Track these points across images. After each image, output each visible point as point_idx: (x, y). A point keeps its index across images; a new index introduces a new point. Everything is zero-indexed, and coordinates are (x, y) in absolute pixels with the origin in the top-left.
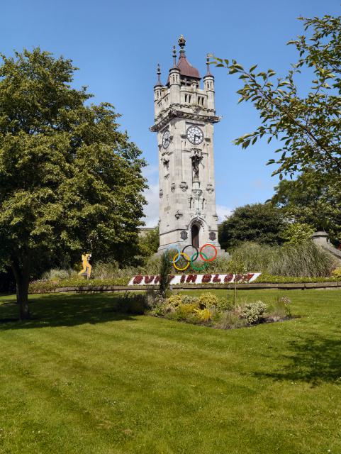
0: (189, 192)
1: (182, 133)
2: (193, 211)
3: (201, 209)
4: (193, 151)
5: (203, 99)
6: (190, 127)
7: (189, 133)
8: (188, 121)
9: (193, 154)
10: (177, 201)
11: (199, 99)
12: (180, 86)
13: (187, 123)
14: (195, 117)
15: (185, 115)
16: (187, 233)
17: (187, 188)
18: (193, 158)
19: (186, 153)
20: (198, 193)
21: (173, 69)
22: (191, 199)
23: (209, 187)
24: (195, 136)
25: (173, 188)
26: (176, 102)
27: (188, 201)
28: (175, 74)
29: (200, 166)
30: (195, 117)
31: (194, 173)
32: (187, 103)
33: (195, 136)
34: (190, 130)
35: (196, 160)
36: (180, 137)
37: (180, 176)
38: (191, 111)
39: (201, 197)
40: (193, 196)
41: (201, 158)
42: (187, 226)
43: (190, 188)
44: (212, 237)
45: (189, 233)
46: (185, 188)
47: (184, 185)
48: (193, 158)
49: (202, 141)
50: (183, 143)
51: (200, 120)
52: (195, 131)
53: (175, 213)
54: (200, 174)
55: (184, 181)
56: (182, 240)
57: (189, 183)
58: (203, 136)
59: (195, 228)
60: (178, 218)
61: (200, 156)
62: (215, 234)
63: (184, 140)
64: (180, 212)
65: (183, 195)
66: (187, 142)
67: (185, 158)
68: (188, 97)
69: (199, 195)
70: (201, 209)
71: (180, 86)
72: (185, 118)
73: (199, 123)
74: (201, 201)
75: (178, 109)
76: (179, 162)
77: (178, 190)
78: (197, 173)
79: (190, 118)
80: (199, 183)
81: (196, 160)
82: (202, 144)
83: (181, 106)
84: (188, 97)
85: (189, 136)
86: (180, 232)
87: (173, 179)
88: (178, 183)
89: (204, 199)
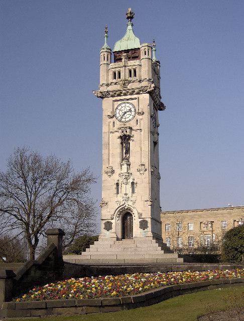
0: (116, 177)
3: (130, 194)
7: (118, 111)
9: (119, 134)
17: (113, 172)
18: (121, 137)
20: (124, 177)
32: (114, 81)
34: (120, 108)
35: (125, 139)
38: (118, 87)
41: (129, 137)
45: (116, 223)
50: (111, 124)
63: (112, 120)
69: (127, 179)
72: (113, 96)
79: (119, 95)
81: (125, 139)
89: (133, 183)
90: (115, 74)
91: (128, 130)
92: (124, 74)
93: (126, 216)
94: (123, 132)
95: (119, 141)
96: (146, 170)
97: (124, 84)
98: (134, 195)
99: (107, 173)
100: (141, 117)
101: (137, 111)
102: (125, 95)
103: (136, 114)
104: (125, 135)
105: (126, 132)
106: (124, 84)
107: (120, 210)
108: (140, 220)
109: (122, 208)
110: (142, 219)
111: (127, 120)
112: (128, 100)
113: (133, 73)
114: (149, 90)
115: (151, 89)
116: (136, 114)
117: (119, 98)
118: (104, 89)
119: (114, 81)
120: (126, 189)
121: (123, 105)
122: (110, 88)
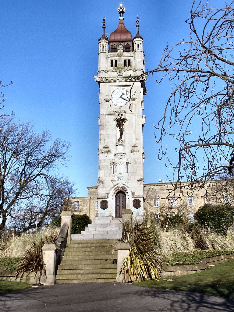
0: (111, 157)
4: (117, 114)
5: (129, 61)
17: (109, 152)
18: (117, 120)
19: (110, 116)
35: (120, 122)
38: (115, 74)
48: (117, 120)
57: (112, 147)
62: (139, 201)
65: (104, 160)
72: (109, 82)
79: (115, 81)
81: (120, 122)
90: (112, 61)
92: (121, 63)
93: (121, 193)
94: (119, 115)
95: (115, 123)
97: (120, 72)
99: (104, 153)
105: (122, 115)
108: (133, 199)
109: (118, 187)
110: (135, 198)
112: (123, 86)
113: (128, 63)
118: (103, 75)
119: (112, 68)
120: (121, 168)
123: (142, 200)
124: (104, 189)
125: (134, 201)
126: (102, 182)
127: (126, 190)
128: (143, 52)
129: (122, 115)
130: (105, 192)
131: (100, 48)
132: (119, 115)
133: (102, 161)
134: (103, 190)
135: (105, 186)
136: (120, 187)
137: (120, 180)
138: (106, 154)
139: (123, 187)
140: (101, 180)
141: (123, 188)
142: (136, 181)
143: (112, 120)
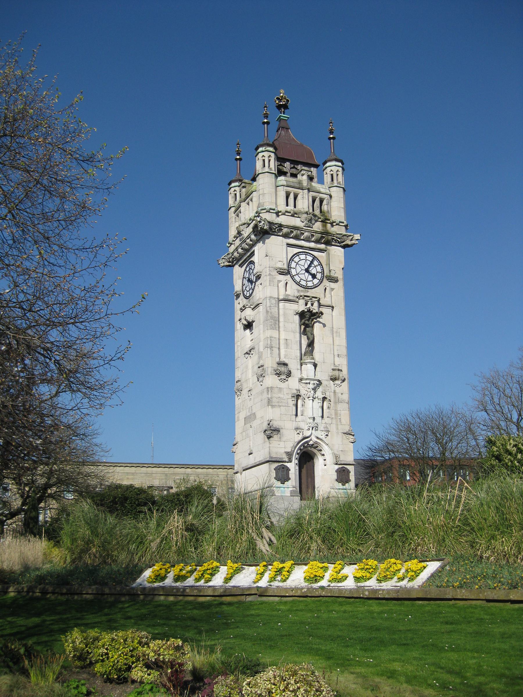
0: (293, 383)
1: (280, 265)
2: (304, 422)
3: (318, 420)
6: (297, 254)
7: (293, 265)
8: (292, 241)
9: (301, 307)
10: (269, 402)
11: (314, 201)
12: (276, 177)
13: (289, 245)
14: (306, 234)
15: (285, 230)
16: (288, 470)
18: (302, 315)
19: (288, 305)
20: (311, 386)
21: (262, 146)
22: (298, 396)
23: (336, 373)
24: (307, 270)
25: (261, 377)
26: (268, 207)
27: (291, 403)
28: (266, 154)
29: (317, 327)
30: (306, 234)
31: (305, 342)
32: (291, 208)
33: (307, 270)
34: (297, 259)
35: (308, 319)
36: (275, 273)
37: (276, 351)
38: (297, 222)
39: (319, 394)
40: (303, 392)
42: (289, 455)
43: (296, 374)
44: (342, 476)
46: (283, 371)
47: (283, 369)
48: (302, 315)
49: (321, 281)
50: (282, 285)
51: (317, 242)
52: (304, 261)
53: (265, 426)
54: (316, 345)
55: (283, 359)
56: (278, 484)
57: (294, 365)
58: (323, 272)
59: (306, 457)
60: (269, 437)
61: (315, 308)
62: (348, 472)
64: (276, 424)
66: (290, 282)
67: (285, 314)
68: (292, 197)
70: (318, 420)
71: (276, 177)
72: (286, 236)
73: (312, 245)
74: (317, 404)
75: (271, 217)
76: (274, 322)
77: (271, 380)
78: (311, 344)
79: (297, 238)
80: (315, 365)
82: (321, 288)
83: (277, 214)
84: (292, 197)
85: (293, 272)
86: (276, 465)
87: (260, 357)
88: (270, 363)
89: (324, 399)
91: (316, 304)
94: (306, 305)
95: (297, 317)
96: (344, 381)
98: (326, 419)
99: (279, 374)
100: (333, 285)
101: (326, 272)
102: (307, 240)
103: (325, 279)
104: (309, 311)
105: (312, 305)
106: (310, 220)
107: (301, 446)
108: (337, 467)
111: (310, 284)
114: (348, 242)
115: (353, 242)
116: (325, 279)
117: (292, 241)
120: (311, 408)
121: (303, 257)
122: (283, 220)
123: (351, 468)
124: (282, 444)
125: (338, 471)
126: (277, 430)
127: (321, 450)
128: (344, 190)
129: (312, 305)
130: (283, 451)
131: (259, 164)
132: (306, 305)
133: (276, 390)
134: (279, 446)
135: (284, 439)
136: (311, 443)
137: (311, 429)
138: (283, 377)
139: (316, 443)
140: (274, 426)
141: (315, 446)
142: (340, 434)
143: (292, 313)
